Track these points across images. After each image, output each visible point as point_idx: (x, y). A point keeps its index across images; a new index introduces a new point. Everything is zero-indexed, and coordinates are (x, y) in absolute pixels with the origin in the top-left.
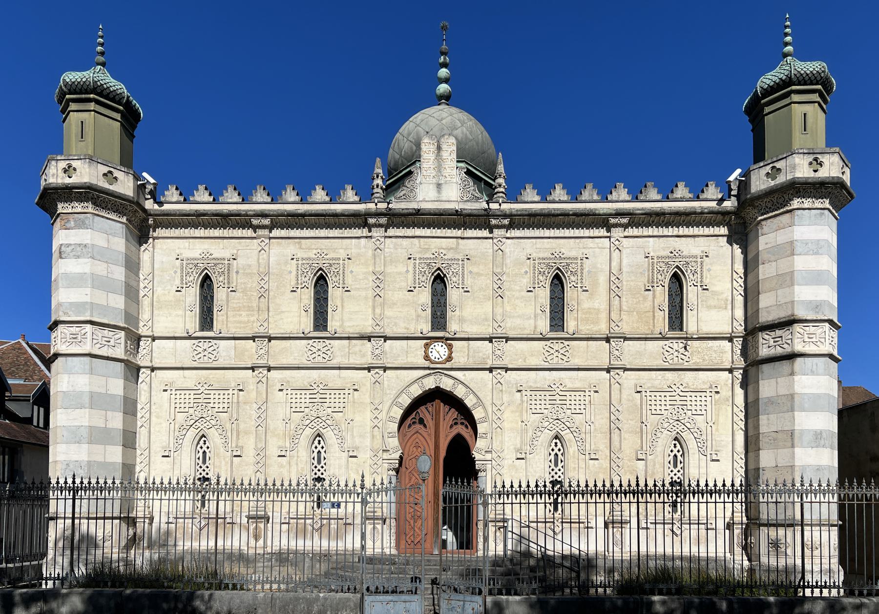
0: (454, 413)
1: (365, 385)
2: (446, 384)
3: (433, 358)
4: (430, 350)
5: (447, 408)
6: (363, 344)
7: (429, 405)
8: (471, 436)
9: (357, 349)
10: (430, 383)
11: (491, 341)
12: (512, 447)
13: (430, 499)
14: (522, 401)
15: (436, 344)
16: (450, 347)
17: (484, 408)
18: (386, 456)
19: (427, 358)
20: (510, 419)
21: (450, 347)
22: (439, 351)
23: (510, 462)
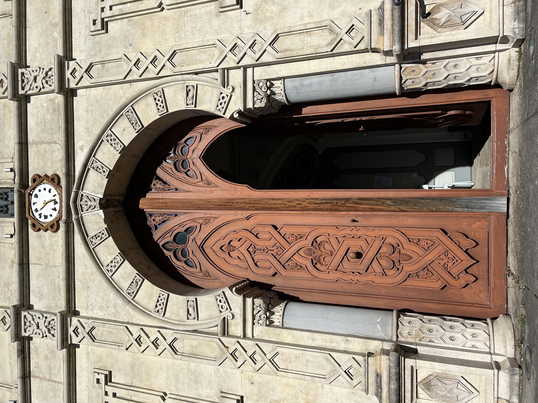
0: (165, 170)
1: (100, 359)
2: (96, 185)
3: (55, 214)
4: (42, 219)
5: (156, 184)
6: (37, 349)
7: (151, 222)
8: (208, 130)
9: (43, 364)
10: (95, 220)
11: (27, 98)
12: (216, 22)
13: (347, 221)
14: (122, 16)
15: (34, 207)
16: (39, 180)
17: (136, 99)
18: (236, 328)
19: (54, 227)
20: (155, 37)
21: (39, 180)
22: (45, 202)
23: (248, 20)
